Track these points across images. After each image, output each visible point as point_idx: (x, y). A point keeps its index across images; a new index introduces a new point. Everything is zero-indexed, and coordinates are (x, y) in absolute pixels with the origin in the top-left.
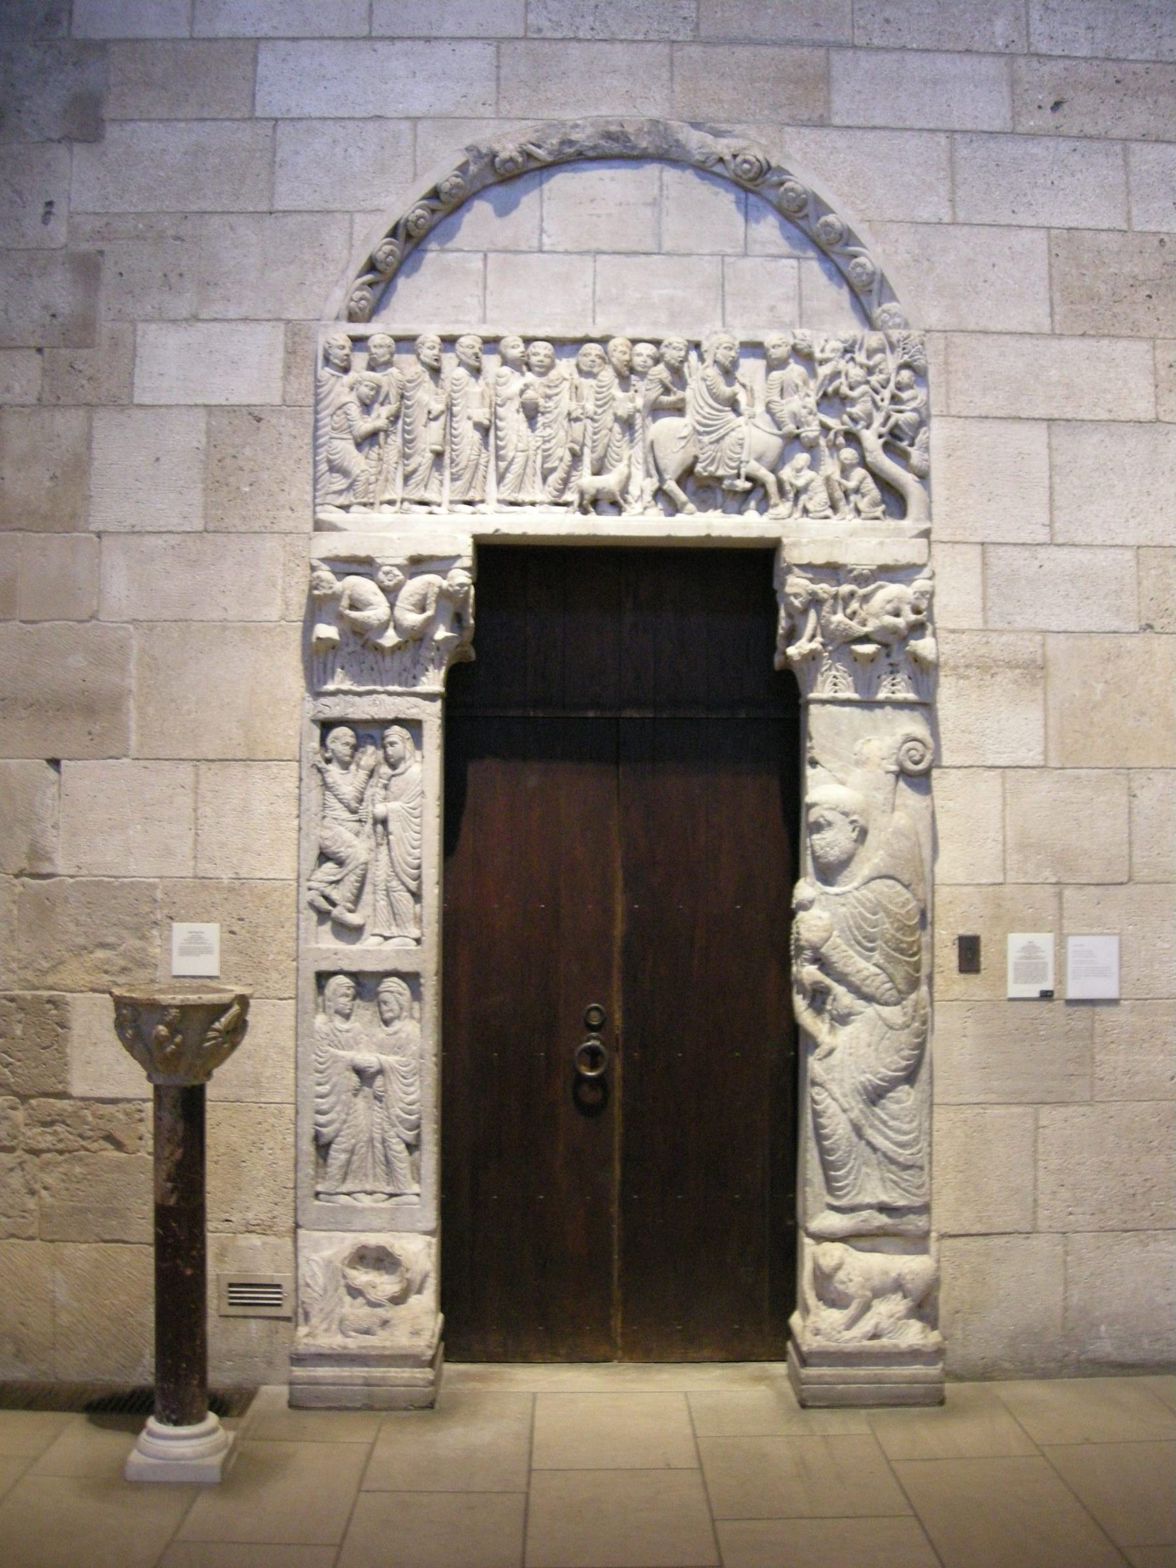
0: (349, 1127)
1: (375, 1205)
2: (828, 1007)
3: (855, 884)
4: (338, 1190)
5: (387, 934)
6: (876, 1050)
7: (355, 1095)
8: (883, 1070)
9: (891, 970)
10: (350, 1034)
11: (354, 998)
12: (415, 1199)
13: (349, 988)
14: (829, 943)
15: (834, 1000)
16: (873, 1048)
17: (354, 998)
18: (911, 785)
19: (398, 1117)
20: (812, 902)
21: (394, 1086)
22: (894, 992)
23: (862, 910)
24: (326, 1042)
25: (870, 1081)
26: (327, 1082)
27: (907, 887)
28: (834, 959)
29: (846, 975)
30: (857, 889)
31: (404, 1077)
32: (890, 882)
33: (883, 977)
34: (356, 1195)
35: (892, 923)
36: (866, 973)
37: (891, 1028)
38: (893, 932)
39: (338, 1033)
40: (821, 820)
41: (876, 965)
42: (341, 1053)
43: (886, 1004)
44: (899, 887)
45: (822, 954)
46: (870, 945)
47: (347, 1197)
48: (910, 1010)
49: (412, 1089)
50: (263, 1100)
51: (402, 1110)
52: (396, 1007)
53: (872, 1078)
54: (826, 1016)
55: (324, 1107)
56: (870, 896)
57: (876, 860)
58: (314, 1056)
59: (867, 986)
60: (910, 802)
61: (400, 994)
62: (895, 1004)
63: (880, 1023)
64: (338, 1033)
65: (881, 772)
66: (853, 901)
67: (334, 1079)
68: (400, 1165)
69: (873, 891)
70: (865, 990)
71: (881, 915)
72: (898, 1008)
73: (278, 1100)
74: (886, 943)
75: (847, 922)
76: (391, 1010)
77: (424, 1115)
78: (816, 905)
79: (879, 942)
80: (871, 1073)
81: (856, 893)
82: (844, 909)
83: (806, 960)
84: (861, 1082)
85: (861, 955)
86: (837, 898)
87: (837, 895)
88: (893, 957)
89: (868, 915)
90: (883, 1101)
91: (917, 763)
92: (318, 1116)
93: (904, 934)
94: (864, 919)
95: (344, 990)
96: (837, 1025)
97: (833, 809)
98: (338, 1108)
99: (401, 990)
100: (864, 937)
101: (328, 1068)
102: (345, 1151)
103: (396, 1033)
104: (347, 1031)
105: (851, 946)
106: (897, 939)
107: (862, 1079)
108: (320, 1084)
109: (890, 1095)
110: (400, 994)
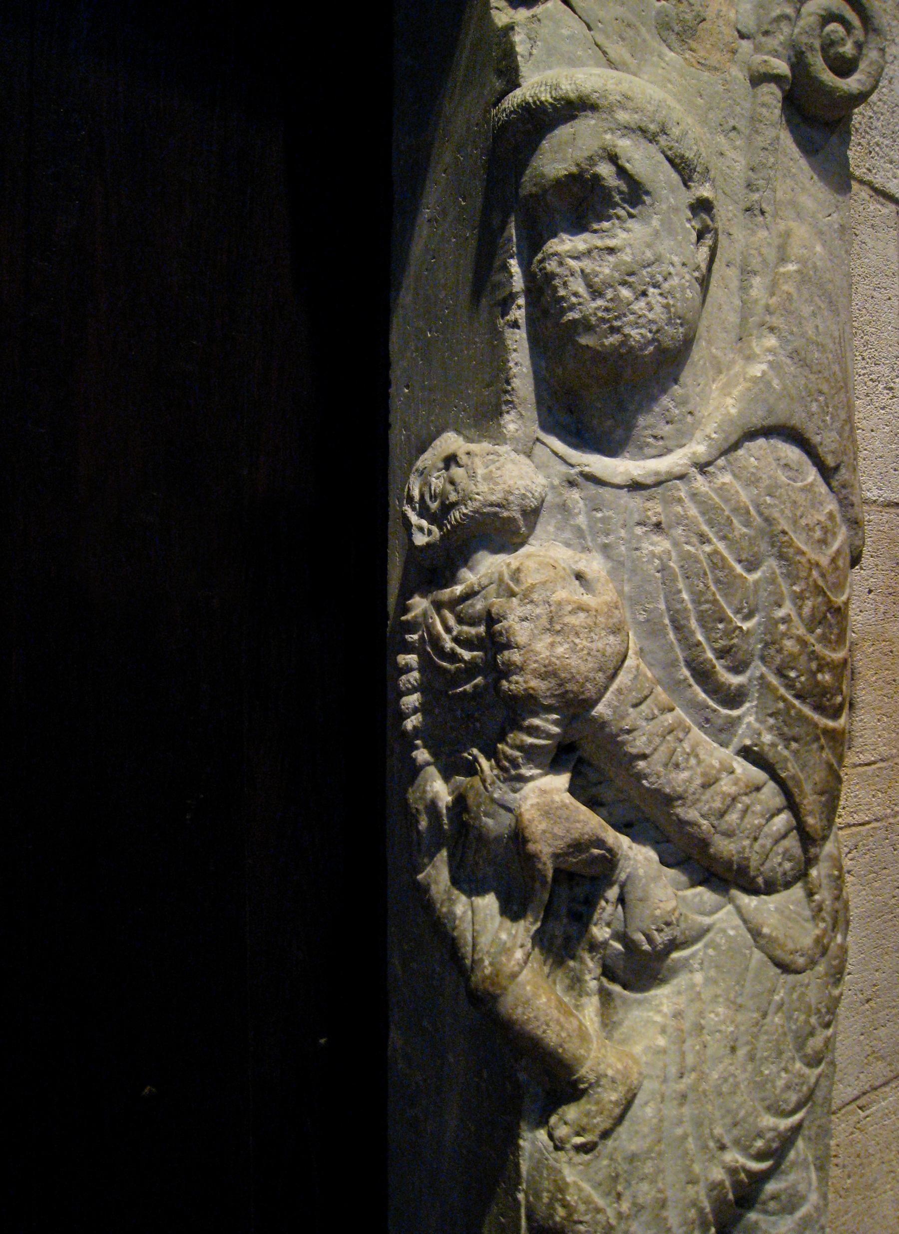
2: (601, 933)
3: (699, 448)
6: (751, 1058)
8: (768, 1121)
9: (790, 769)
14: (623, 679)
15: (621, 900)
16: (742, 1052)
18: (808, 148)
20: (532, 514)
22: (792, 843)
23: (721, 546)
25: (733, 1171)
27: (827, 472)
28: (638, 743)
29: (669, 800)
30: (703, 467)
32: (792, 453)
33: (770, 794)
35: (798, 599)
36: (726, 786)
37: (785, 968)
38: (801, 631)
40: (605, 170)
41: (746, 753)
43: (770, 888)
44: (812, 475)
45: (602, 724)
46: (735, 680)
48: (824, 896)
53: (742, 1160)
54: (591, 965)
56: (745, 497)
57: (757, 369)
59: (729, 834)
60: (807, 202)
62: (788, 885)
63: (758, 955)
65: (738, 74)
66: (693, 511)
69: (752, 481)
70: (724, 847)
71: (771, 564)
72: (797, 891)
74: (780, 673)
75: (672, 595)
78: (546, 527)
79: (758, 668)
80: (737, 1142)
81: (700, 483)
82: (661, 544)
83: (530, 753)
84: (716, 1186)
85: (706, 722)
86: (635, 502)
87: (635, 486)
88: (802, 719)
89: (739, 569)
90: (753, 1216)
91: (844, 67)
93: (824, 639)
94: (728, 583)
96: (617, 988)
97: (652, 138)
100: (722, 654)
105: (676, 687)
106: (814, 656)
107: (718, 1174)
109: (771, 1187)
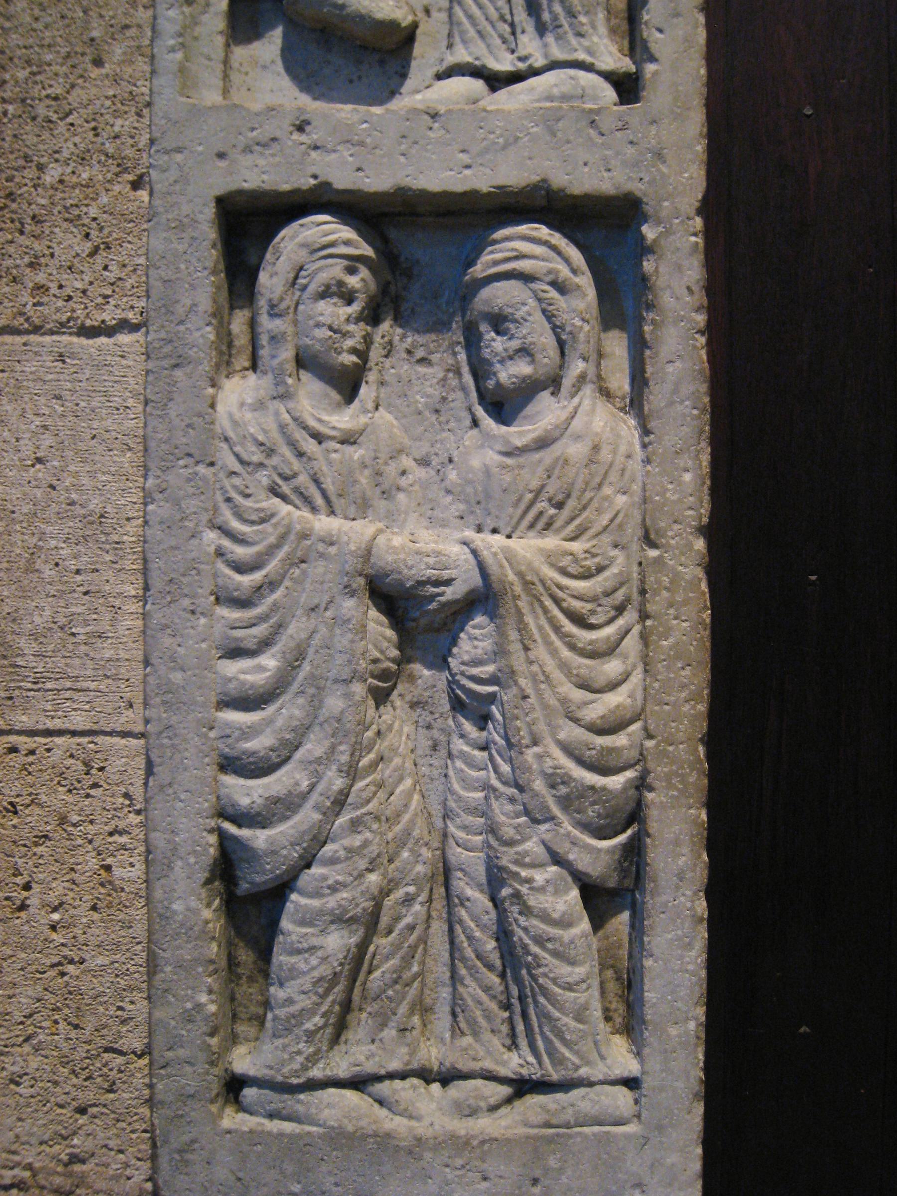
0: (355, 825)
1: (461, 1127)
4: (316, 1073)
5: (504, 64)
7: (381, 697)
10: (356, 453)
11: (372, 316)
12: (623, 1098)
13: (353, 263)
17: (372, 316)
19: (554, 780)
21: (540, 652)
24: (264, 478)
26: (265, 644)
31: (579, 621)
34: (384, 1088)
39: (310, 446)
42: (323, 523)
47: (350, 1095)
49: (613, 667)
50: (24, 720)
51: (567, 749)
52: (546, 340)
55: (259, 744)
58: (211, 537)
61: (560, 287)
64: (310, 446)
67: (296, 630)
68: (564, 971)
73: (79, 721)
76: (525, 352)
77: (659, 770)
92: (230, 780)
95: (335, 270)
98: (313, 747)
99: (564, 271)
101: (272, 584)
102: (341, 919)
103: (542, 443)
104: (349, 439)
108: (235, 652)
110: (560, 287)
